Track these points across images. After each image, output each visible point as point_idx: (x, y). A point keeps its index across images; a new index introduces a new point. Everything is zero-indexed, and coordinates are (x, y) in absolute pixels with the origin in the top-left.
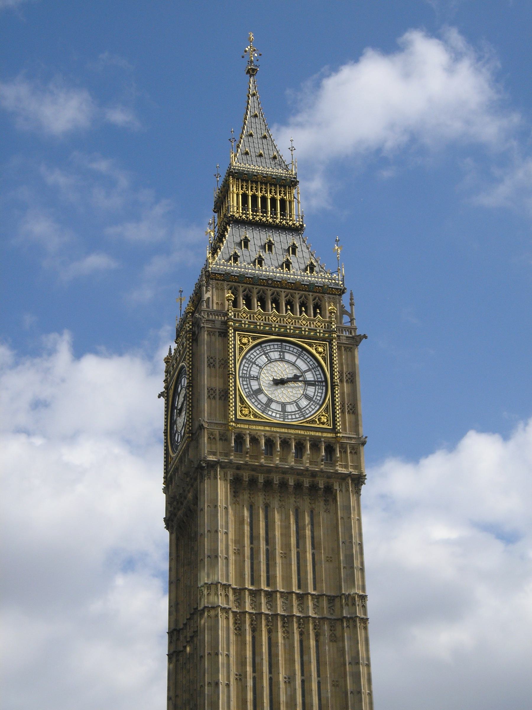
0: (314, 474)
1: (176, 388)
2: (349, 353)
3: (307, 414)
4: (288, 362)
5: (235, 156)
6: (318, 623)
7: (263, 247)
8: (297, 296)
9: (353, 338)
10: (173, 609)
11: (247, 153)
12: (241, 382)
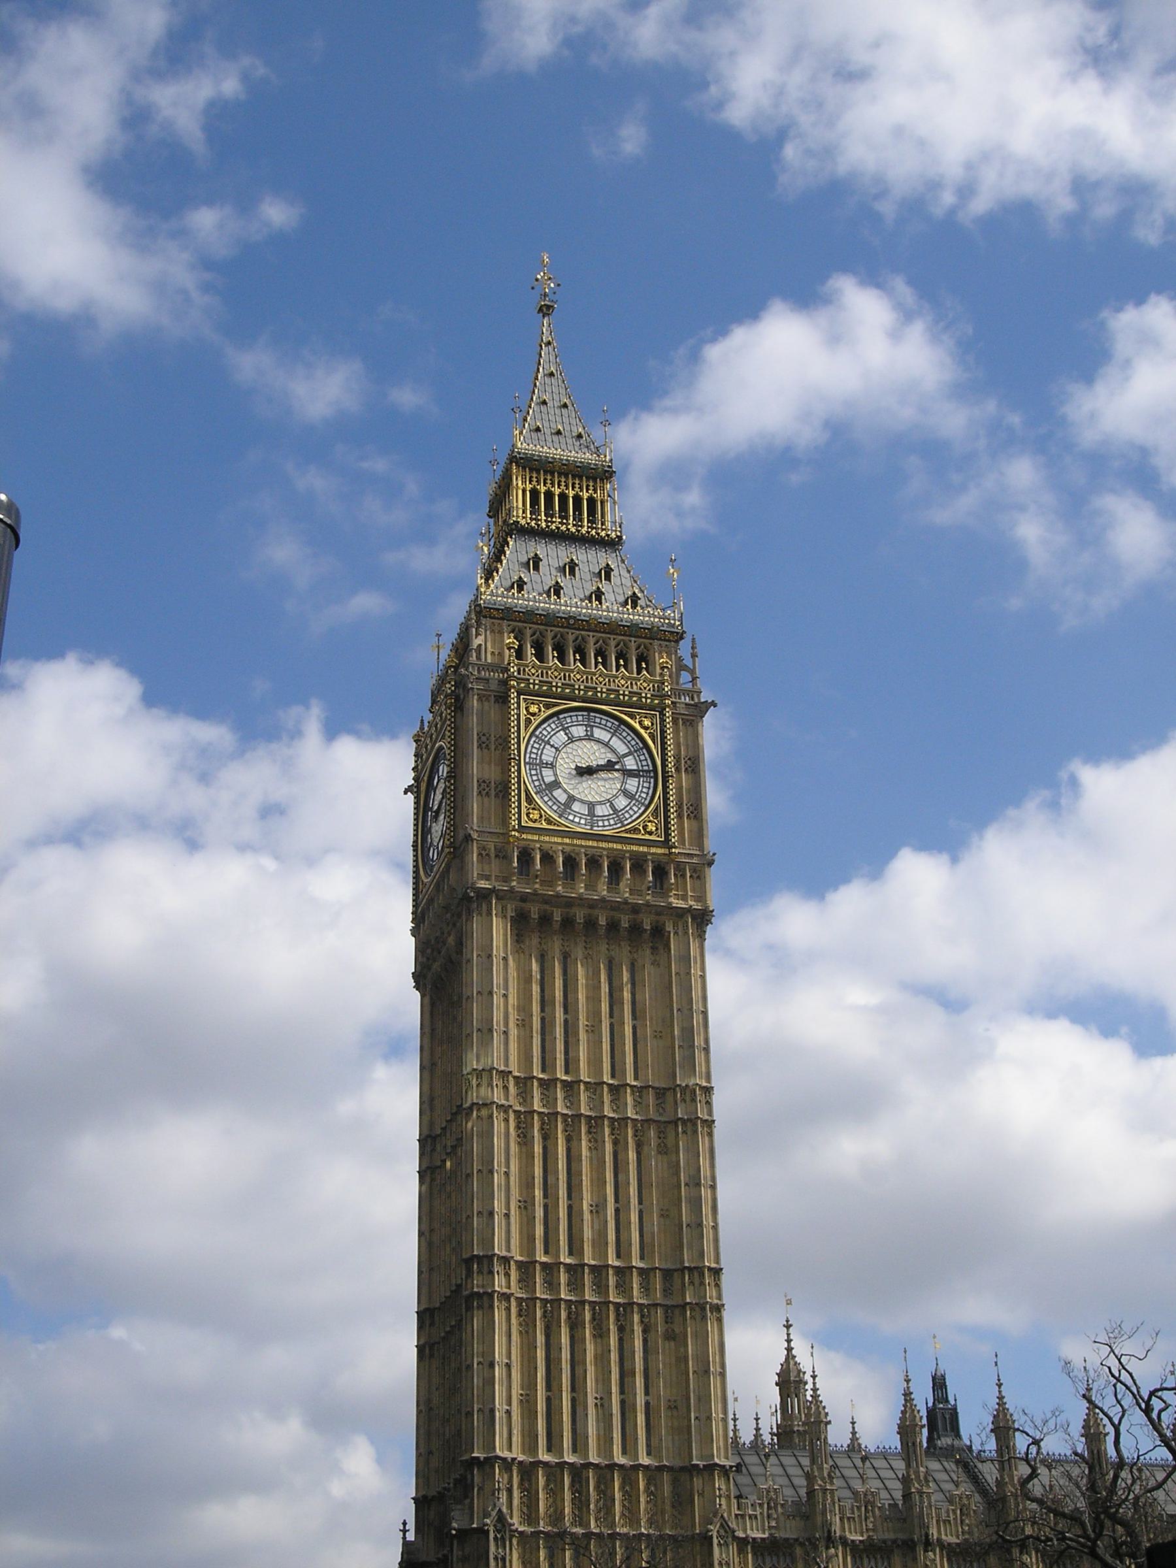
0: (635, 909)
1: (431, 779)
2: (690, 729)
4: (598, 741)
5: (521, 433)
6: (641, 1128)
7: (562, 570)
8: (613, 643)
9: (696, 705)
10: (426, 1106)
11: (538, 430)
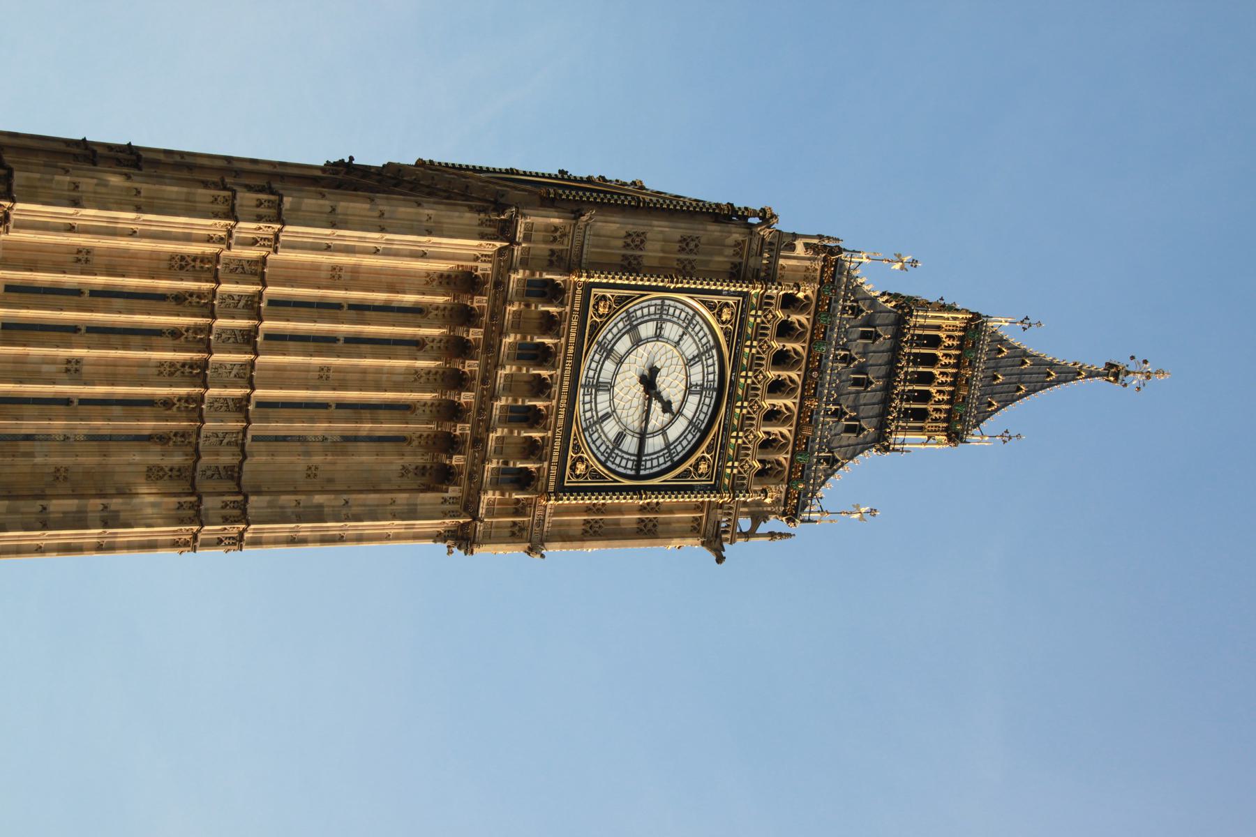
0: (479, 441)
3: (590, 436)
6: (189, 441)
10: (178, 159)
12: (654, 302)
